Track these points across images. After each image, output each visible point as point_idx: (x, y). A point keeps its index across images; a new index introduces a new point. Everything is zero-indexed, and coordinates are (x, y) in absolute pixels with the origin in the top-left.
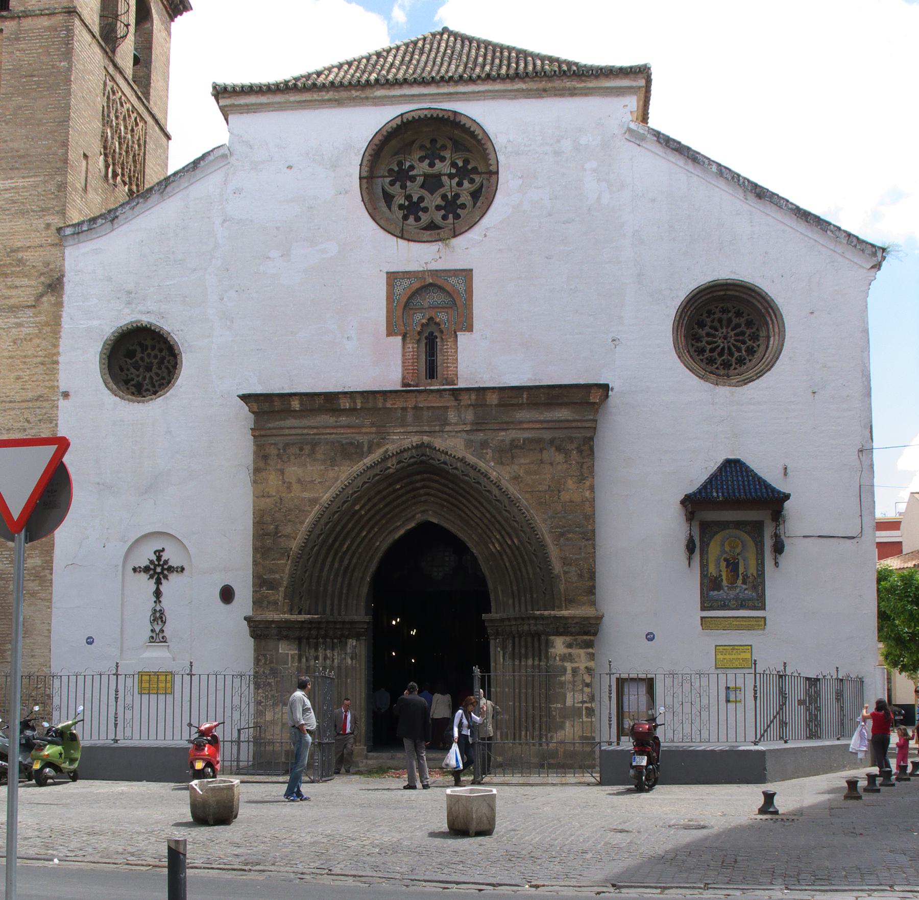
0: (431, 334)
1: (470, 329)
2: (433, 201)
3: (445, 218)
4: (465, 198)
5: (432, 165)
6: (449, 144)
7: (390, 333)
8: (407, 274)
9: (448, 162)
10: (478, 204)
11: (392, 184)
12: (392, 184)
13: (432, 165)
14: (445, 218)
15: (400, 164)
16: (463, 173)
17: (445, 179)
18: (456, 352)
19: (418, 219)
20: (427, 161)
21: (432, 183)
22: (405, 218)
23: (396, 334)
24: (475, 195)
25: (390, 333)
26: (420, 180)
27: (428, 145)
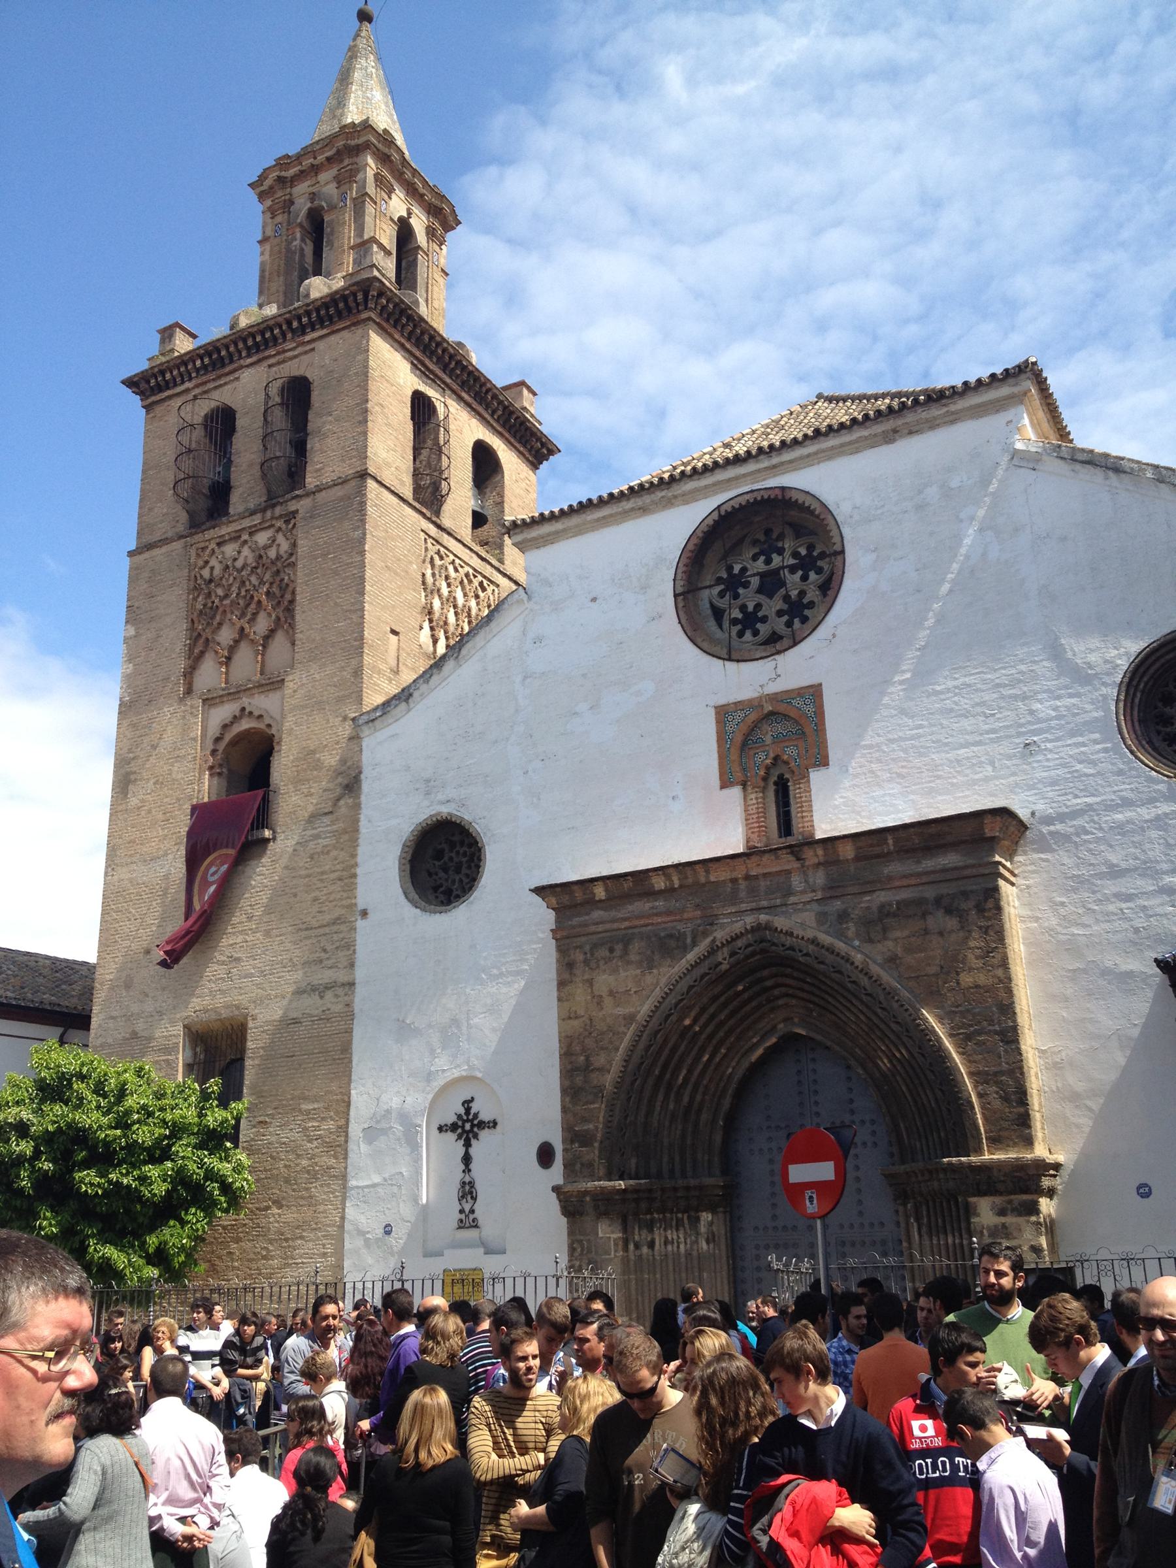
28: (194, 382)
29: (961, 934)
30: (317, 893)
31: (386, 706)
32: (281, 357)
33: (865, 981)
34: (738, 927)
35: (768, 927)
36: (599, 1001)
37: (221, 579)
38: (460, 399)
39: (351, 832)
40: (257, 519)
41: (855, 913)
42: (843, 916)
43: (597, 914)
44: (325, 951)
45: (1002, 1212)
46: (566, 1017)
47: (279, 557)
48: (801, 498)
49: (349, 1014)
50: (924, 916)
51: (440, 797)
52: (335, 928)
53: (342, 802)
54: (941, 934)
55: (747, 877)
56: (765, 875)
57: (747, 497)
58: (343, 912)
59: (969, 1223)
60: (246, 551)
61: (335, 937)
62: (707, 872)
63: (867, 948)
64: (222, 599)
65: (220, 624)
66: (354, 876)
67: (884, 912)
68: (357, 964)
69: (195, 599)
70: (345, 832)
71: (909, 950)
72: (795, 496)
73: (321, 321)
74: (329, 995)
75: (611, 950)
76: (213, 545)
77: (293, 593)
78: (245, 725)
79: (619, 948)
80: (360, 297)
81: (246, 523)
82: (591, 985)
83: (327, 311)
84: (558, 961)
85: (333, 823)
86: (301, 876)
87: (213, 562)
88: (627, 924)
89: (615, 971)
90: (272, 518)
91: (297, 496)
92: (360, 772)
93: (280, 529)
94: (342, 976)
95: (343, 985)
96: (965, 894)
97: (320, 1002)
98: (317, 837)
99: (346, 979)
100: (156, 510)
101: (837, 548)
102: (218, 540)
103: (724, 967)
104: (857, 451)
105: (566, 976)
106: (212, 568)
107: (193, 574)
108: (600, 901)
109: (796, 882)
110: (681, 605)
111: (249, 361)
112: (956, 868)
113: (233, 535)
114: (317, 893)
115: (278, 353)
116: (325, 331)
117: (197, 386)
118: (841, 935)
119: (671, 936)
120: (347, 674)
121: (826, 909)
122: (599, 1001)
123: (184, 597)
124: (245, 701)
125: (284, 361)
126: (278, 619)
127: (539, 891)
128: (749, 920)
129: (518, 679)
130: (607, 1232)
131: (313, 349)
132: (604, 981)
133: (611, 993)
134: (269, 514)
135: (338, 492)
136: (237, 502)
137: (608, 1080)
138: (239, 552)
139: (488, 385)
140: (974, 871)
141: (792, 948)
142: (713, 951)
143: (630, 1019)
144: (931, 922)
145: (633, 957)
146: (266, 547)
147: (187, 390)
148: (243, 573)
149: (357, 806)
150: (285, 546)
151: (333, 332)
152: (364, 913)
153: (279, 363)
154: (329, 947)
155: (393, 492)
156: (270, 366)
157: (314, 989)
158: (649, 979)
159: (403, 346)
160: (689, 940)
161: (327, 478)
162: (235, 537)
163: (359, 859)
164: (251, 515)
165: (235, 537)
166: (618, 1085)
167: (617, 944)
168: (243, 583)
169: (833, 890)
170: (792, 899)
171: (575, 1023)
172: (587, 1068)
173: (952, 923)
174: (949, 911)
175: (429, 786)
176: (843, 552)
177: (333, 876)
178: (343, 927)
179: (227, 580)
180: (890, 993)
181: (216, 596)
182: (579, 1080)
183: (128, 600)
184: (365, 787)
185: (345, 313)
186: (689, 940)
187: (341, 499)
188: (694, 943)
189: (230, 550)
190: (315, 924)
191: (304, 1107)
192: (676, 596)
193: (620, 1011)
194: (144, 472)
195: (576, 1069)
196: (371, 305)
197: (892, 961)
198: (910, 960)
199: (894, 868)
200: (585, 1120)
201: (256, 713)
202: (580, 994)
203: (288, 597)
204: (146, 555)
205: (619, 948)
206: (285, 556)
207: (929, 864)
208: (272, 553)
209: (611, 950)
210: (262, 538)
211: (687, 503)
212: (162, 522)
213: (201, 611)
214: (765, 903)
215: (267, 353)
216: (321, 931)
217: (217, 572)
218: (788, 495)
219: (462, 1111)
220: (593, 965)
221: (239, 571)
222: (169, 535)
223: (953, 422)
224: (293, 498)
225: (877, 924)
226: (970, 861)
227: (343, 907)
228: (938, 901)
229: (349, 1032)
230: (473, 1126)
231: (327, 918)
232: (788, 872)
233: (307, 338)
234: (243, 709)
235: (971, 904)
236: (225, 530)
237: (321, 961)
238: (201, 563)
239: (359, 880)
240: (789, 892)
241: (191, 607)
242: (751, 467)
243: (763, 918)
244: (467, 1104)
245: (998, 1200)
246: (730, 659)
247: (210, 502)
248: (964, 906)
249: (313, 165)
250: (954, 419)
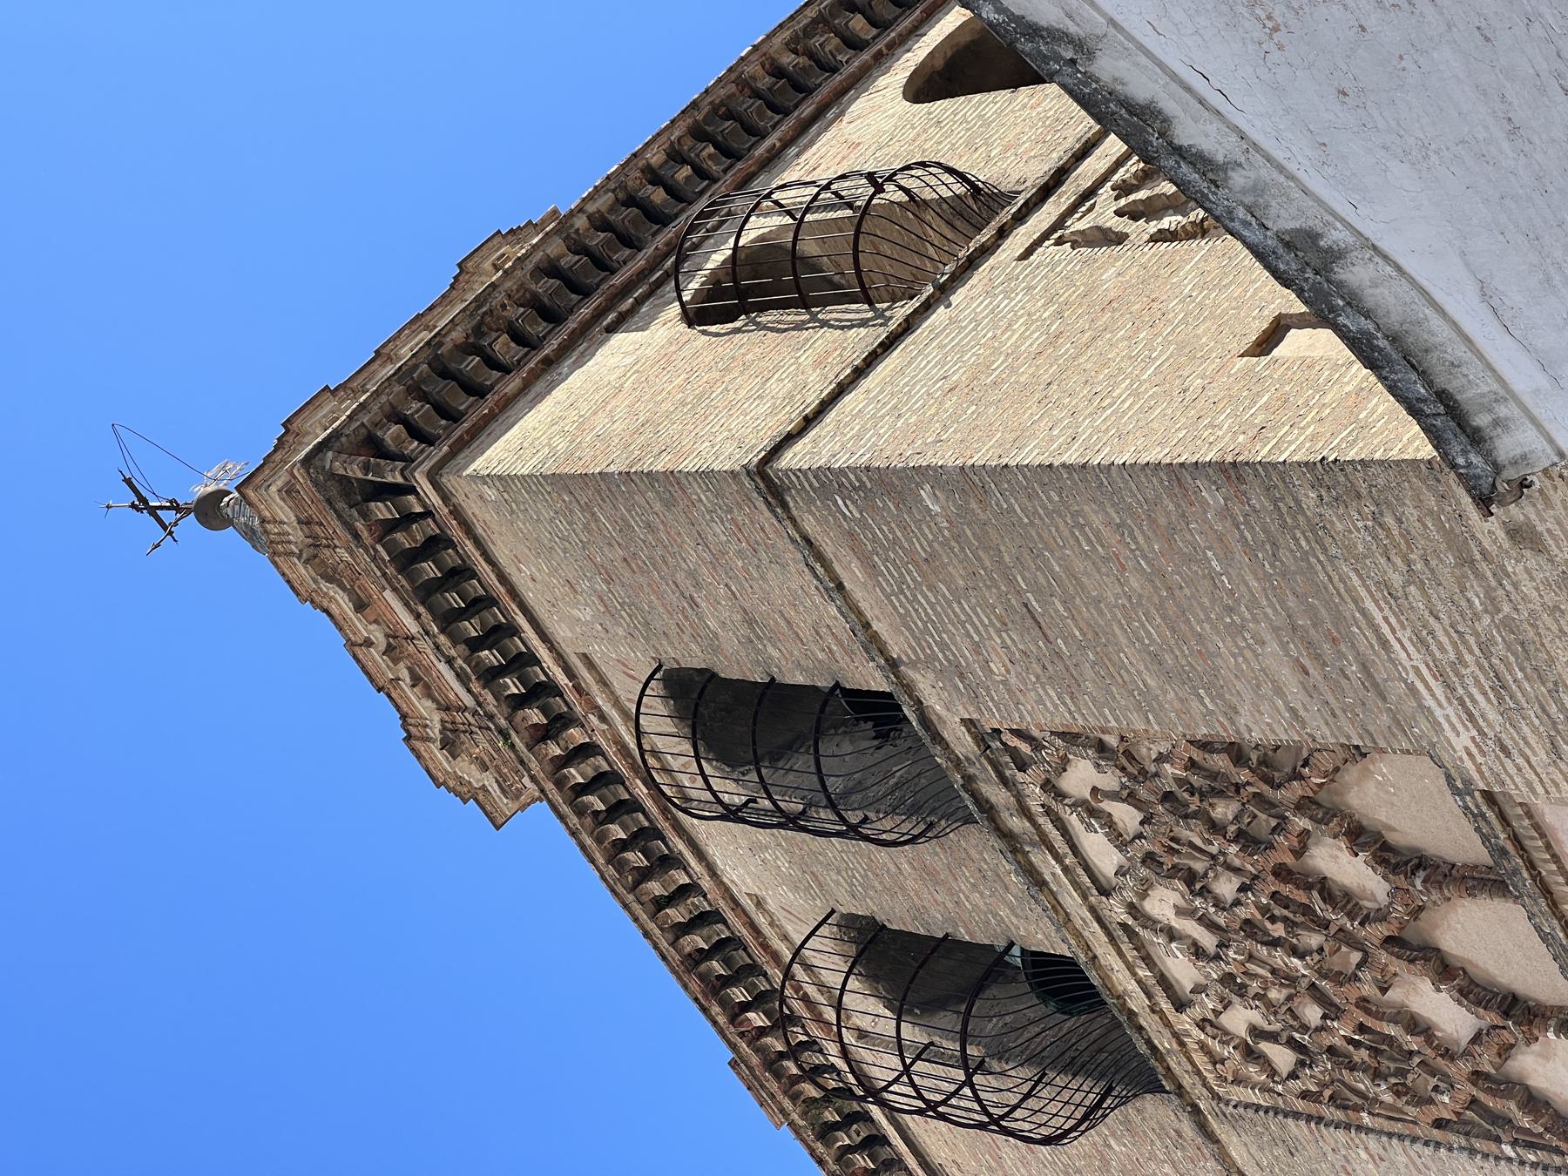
31: (1387, 354)
38: (773, 159)
73: (499, 634)
76: (1184, 1022)
77: (1205, 746)
81: (1071, 900)
83: (462, 614)
93: (1048, 786)
120: (1350, 526)
139: (753, 68)
155: (860, 372)
159: (549, 363)
185: (450, 558)
187: (871, 569)
203: (1220, 762)
249: (389, 650)
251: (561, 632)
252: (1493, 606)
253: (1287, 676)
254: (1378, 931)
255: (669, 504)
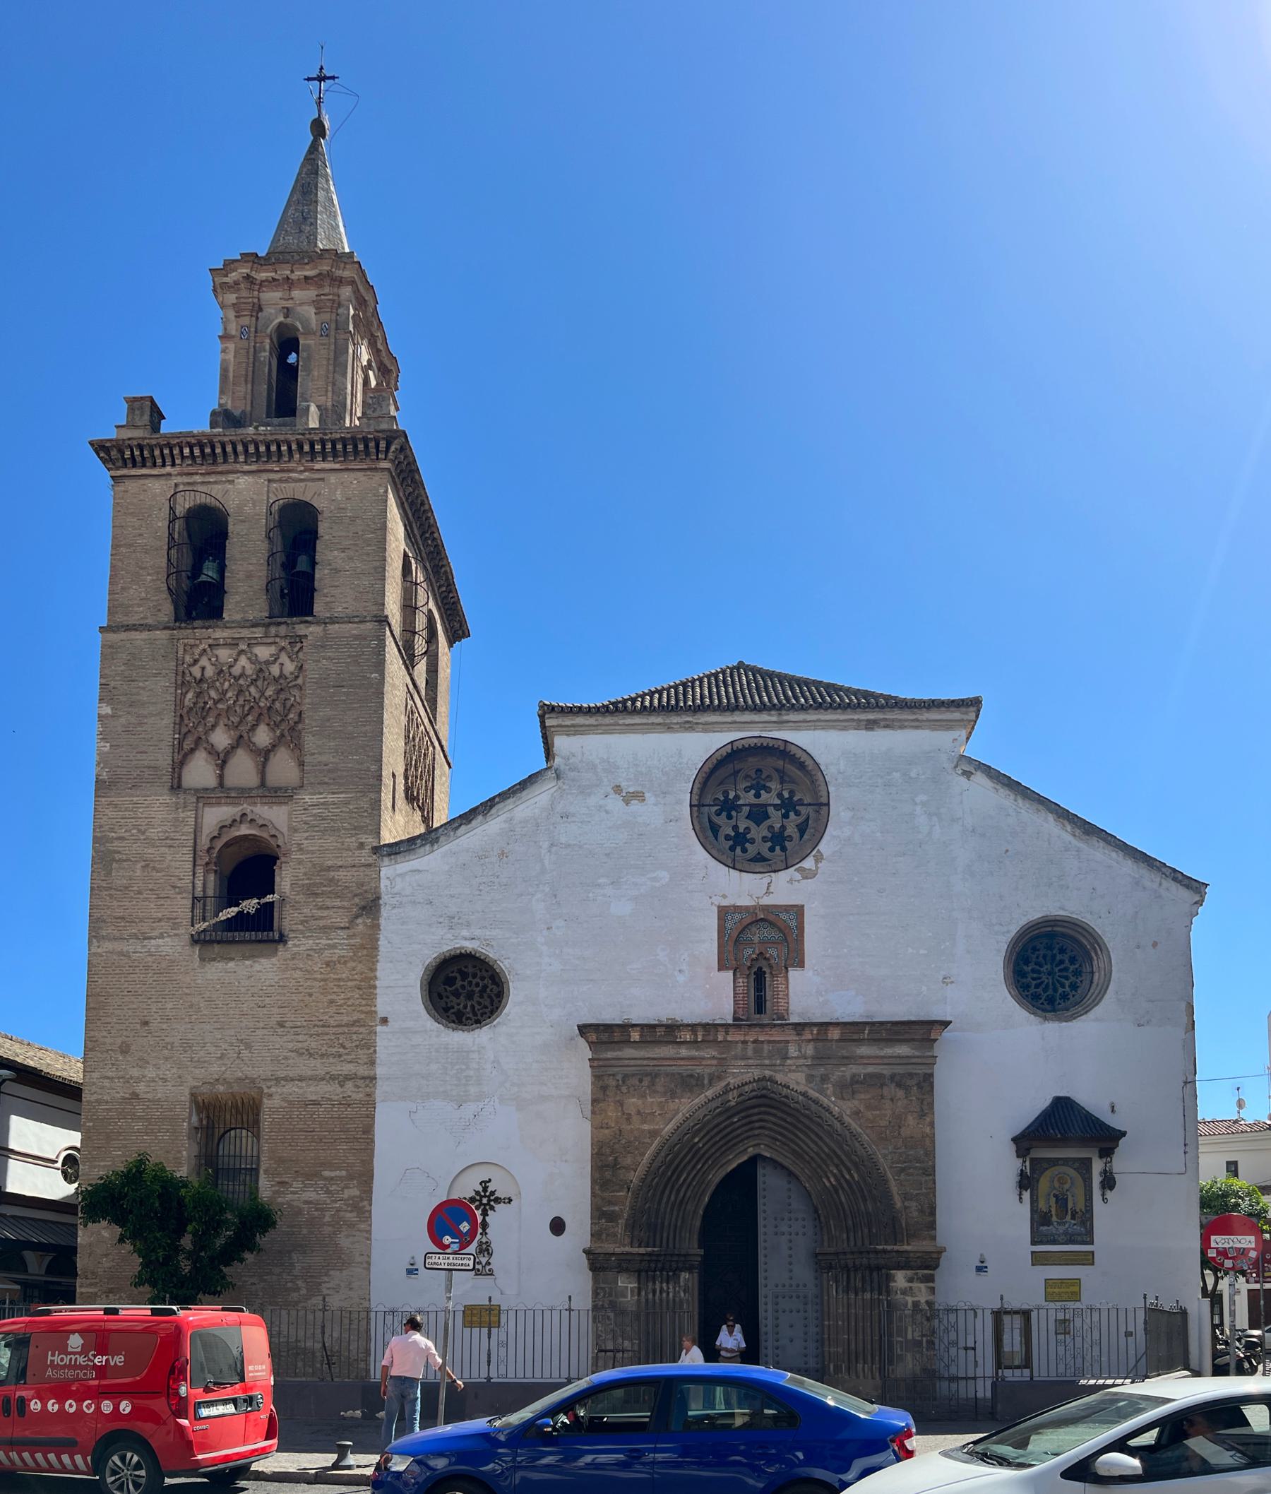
0: (760, 968)
1: (801, 964)
2: (758, 832)
3: (772, 849)
4: (791, 830)
5: (758, 796)
6: (776, 775)
7: (722, 967)
8: (737, 909)
9: (774, 793)
10: (805, 837)
11: (718, 814)
12: (718, 814)
13: (758, 796)
14: (772, 849)
15: (726, 793)
16: (788, 806)
17: (771, 810)
18: (787, 988)
19: (744, 851)
20: (753, 792)
21: (758, 815)
22: (732, 849)
23: (727, 969)
24: (802, 829)
25: (722, 967)
26: (746, 810)
27: (754, 776)
28: (177, 469)
29: (905, 1102)
30: (334, 997)
32: (285, 475)
33: (837, 1125)
34: (748, 1077)
35: (771, 1080)
36: (629, 1118)
37: (214, 682)
39: (369, 949)
40: (258, 632)
41: (834, 1078)
42: (825, 1079)
43: (629, 1052)
44: (344, 1047)
45: (911, 1280)
46: (597, 1127)
47: (282, 675)
48: (799, 754)
49: (370, 1103)
50: (882, 1086)
51: (465, 933)
52: (355, 1029)
53: (360, 921)
54: (892, 1100)
55: (755, 1042)
56: (769, 1042)
57: (755, 741)
58: (363, 1016)
59: (888, 1286)
60: (243, 661)
61: (354, 1037)
62: (727, 1033)
63: (840, 1102)
64: (216, 702)
65: (214, 727)
66: (375, 987)
67: (855, 1080)
68: (378, 1061)
69: (184, 695)
70: (363, 947)
71: (869, 1107)
72: (793, 750)
73: (335, 454)
74: (349, 1085)
75: (641, 1081)
78: (244, 830)
79: (646, 1081)
80: (383, 445)
81: (245, 633)
82: (622, 1105)
84: (593, 1083)
85: (349, 937)
86: (315, 979)
87: (204, 662)
88: (655, 1062)
89: (643, 1096)
90: (277, 636)
91: (306, 622)
92: (379, 898)
93: (283, 648)
94: (363, 1071)
95: (363, 1078)
96: (911, 1075)
97: (339, 1090)
98: (334, 947)
99: (366, 1073)
100: (132, 591)
101: (824, 800)
102: (210, 641)
103: (733, 1103)
104: (845, 729)
105: (601, 1096)
106: (203, 669)
107: (181, 669)
108: (635, 1042)
109: (793, 1051)
110: (695, 815)
111: (246, 468)
112: (907, 1057)
113: (229, 641)
114: (334, 997)
115: (282, 471)
116: (337, 466)
117: (180, 474)
118: (822, 1092)
119: (691, 1076)
121: (813, 1073)
122: (629, 1118)
123: (172, 690)
124: (246, 807)
125: (286, 481)
126: (282, 735)
127: (584, 1029)
128: (757, 1073)
129: (546, 845)
130: (626, 1283)
131: (322, 479)
132: (633, 1102)
133: (639, 1113)
134: (273, 630)
135: (353, 629)
136: (232, 608)
137: (635, 1177)
138: (236, 660)
140: (919, 1061)
141: (786, 1097)
142: (727, 1090)
143: (653, 1134)
144: (886, 1091)
145: (659, 1088)
146: (267, 663)
147: (169, 475)
148: (241, 682)
149: (376, 927)
150: (290, 667)
151: (347, 470)
152: (384, 1021)
153: (280, 481)
154: (348, 1045)
156: (269, 481)
157: (333, 1078)
158: (672, 1106)
160: (706, 1082)
161: (339, 610)
162: (233, 644)
163: (378, 974)
164: (253, 626)
165: (233, 644)
166: (643, 1180)
167: (648, 1077)
168: (240, 692)
169: (819, 1059)
170: (789, 1062)
171: (607, 1131)
172: (615, 1166)
173: (900, 1093)
174: (899, 1085)
175: (452, 922)
176: (828, 804)
177: (349, 983)
178: (361, 1030)
179: (222, 684)
180: (854, 1136)
181: (210, 698)
182: (608, 1174)
183: (101, 677)
184: (384, 912)
186: (706, 1082)
187: (356, 637)
188: (710, 1084)
189: (224, 654)
190: (332, 1022)
191: (326, 1173)
192: (691, 806)
193: (646, 1127)
194: (115, 546)
195: (607, 1166)
196: (391, 455)
197: (857, 1114)
198: (869, 1114)
199: (864, 1050)
200: (610, 1203)
201: (261, 822)
202: (612, 1113)
204: (123, 635)
205: (646, 1081)
206: (291, 677)
207: (888, 1051)
208: (275, 670)
209: (641, 1081)
210: (263, 653)
211: (705, 731)
212: (139, 606)
213: (191, 709)
214: (767, 1062)
215: (269, 466)
216: (340, 1030)
217: (210, 672)
218: (790, 747)
219: (480, 1189)
220: (624, 1089)
221: (236, 679)
222: (150, 621)
223: (917, 727)
224: (302, 622)
225: (848, 1088)
226: (917, 1053)
227: (362, 1012)
228: (892, 1077)
229: (372, 1117)
230: (489, 1201)
231: (345, 1019)
232: (787, 1042)
233: (317, 466)
234: (244, 815)
235: (914, 1082)
236: (219, 634)
237: (340, 1056)
238: (188, 659)
239: (378, 991)
240: (785, 1057)
241: (179, 702)
242: (764, 717)
243: (768, 1073)
244: (485, 1184)
245: (910, 1273)
246: (734, 868)
247: (199, 600)
248: (909, 1083)
250: (917, 724)
251: (333, 478)
252: (345, 829)
253: (324, 758)
254: (245, 735)
255: (375, 568)
